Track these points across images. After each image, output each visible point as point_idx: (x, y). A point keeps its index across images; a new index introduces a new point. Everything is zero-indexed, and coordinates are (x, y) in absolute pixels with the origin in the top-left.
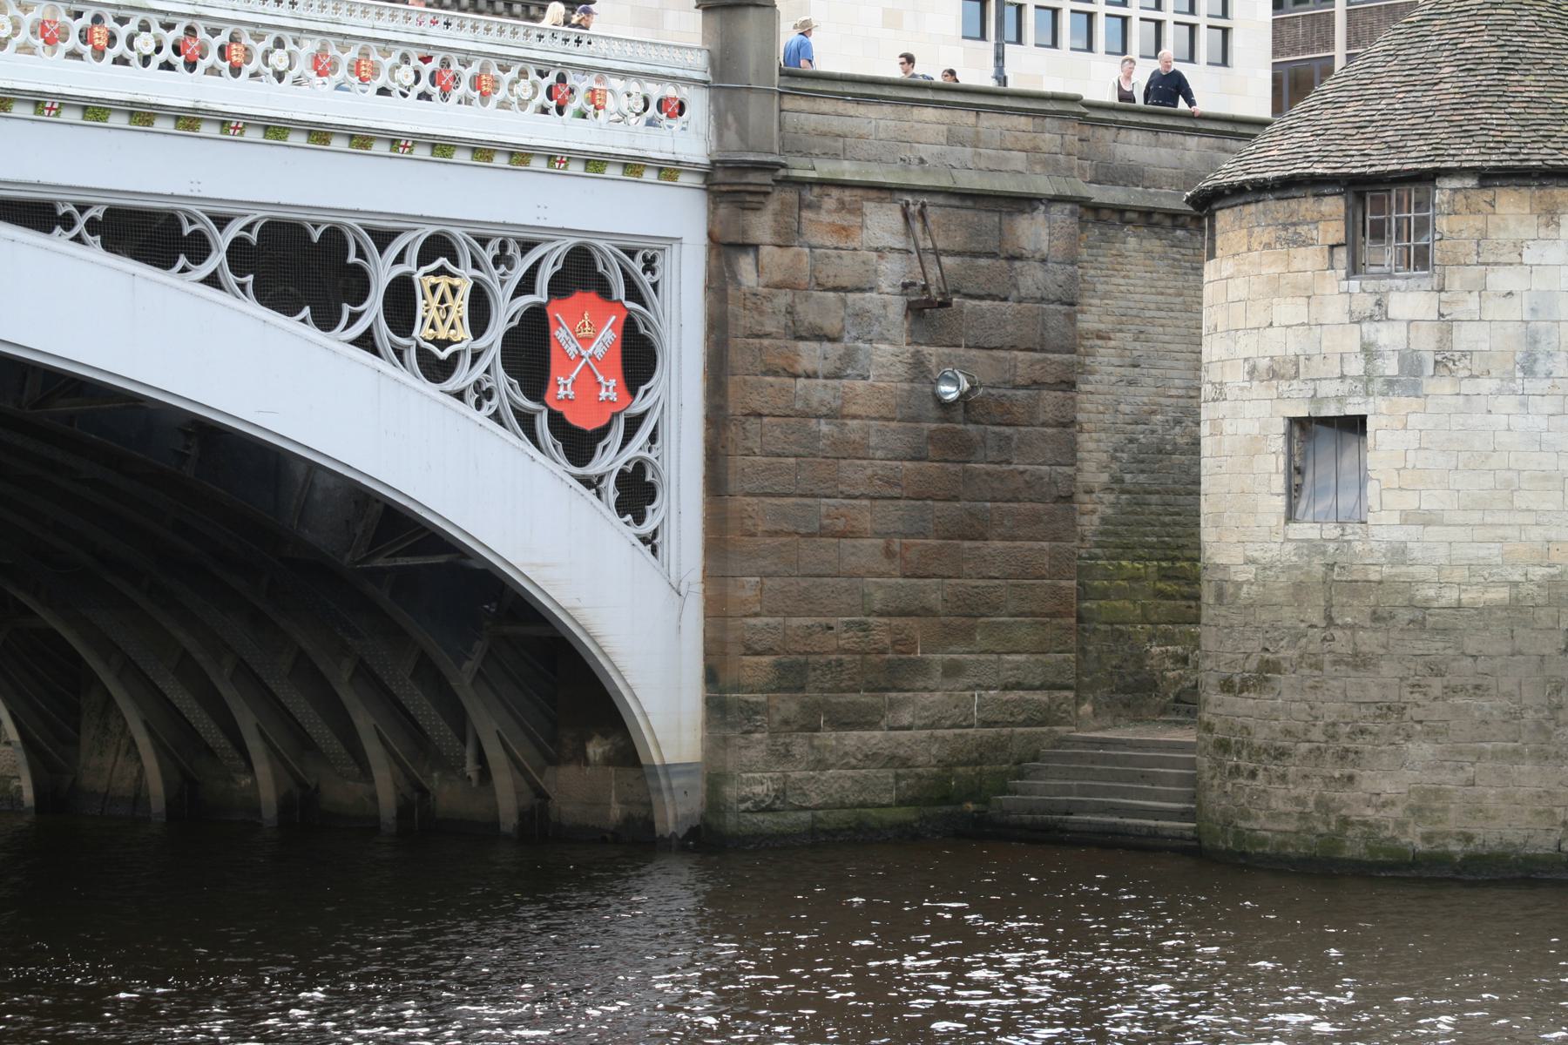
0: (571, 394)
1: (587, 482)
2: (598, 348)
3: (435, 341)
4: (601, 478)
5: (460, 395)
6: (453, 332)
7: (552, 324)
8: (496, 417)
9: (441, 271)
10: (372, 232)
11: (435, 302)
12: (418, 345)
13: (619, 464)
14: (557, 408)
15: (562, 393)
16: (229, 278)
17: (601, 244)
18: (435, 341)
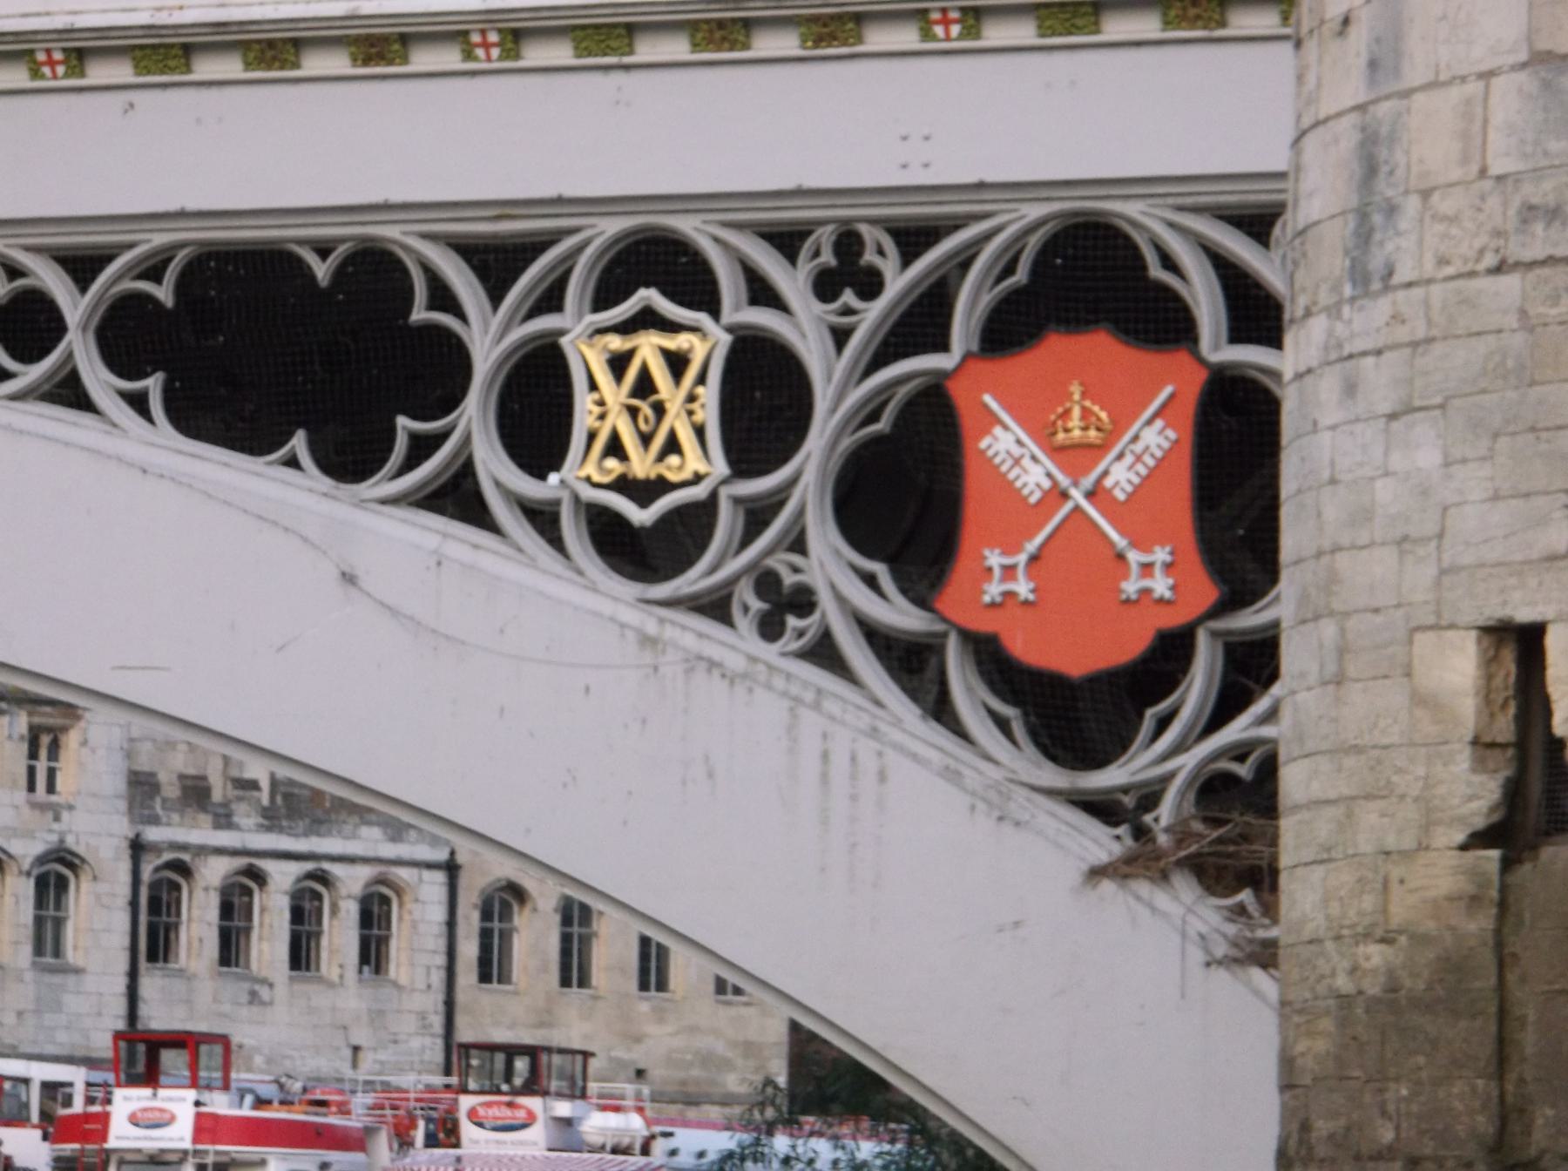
0: (1023, 588)
1: (1101, 808)
2: (1121, 476)
3: (624, 485)
4: (1149, 797)
5: (716, 607)
6: (674, 460)
7: (967, 420)
8: (824, 653)
9: (647, 320)
10: (468, 250)
11: (615, 394)
12: (576, 499)
13: (1189, 761)
14: (983, 624)
15: (993, 590)
16: (98, 379)
17: (1132, 209)
18: (624, 485)
